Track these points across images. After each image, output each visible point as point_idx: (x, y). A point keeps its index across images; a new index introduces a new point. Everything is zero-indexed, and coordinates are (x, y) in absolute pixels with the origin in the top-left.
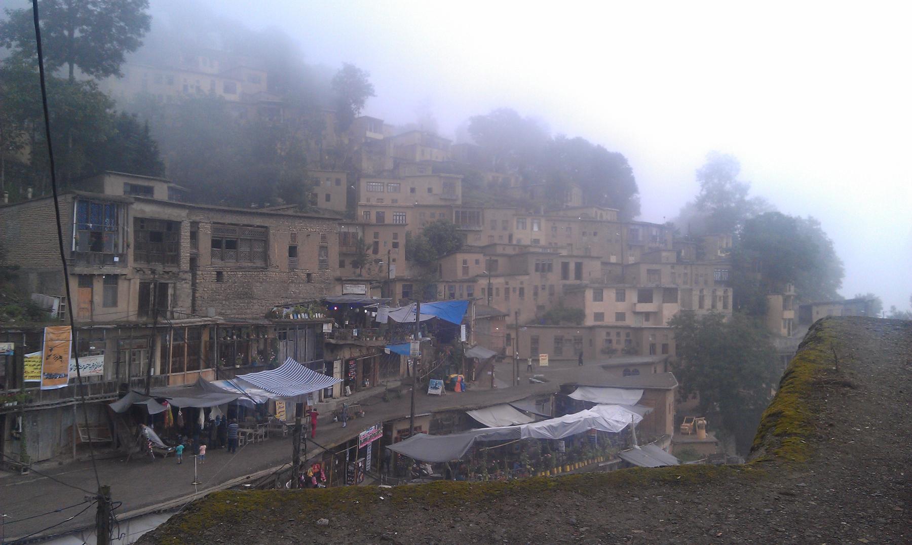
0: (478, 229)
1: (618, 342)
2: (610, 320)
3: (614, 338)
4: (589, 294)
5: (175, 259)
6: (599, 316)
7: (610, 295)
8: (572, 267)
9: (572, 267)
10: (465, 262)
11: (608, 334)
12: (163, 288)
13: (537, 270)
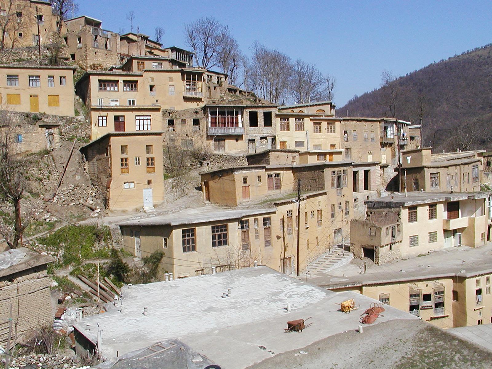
4: (405, 213)
7: (422, 212)
8: (361, 176)
10: (245, 180)
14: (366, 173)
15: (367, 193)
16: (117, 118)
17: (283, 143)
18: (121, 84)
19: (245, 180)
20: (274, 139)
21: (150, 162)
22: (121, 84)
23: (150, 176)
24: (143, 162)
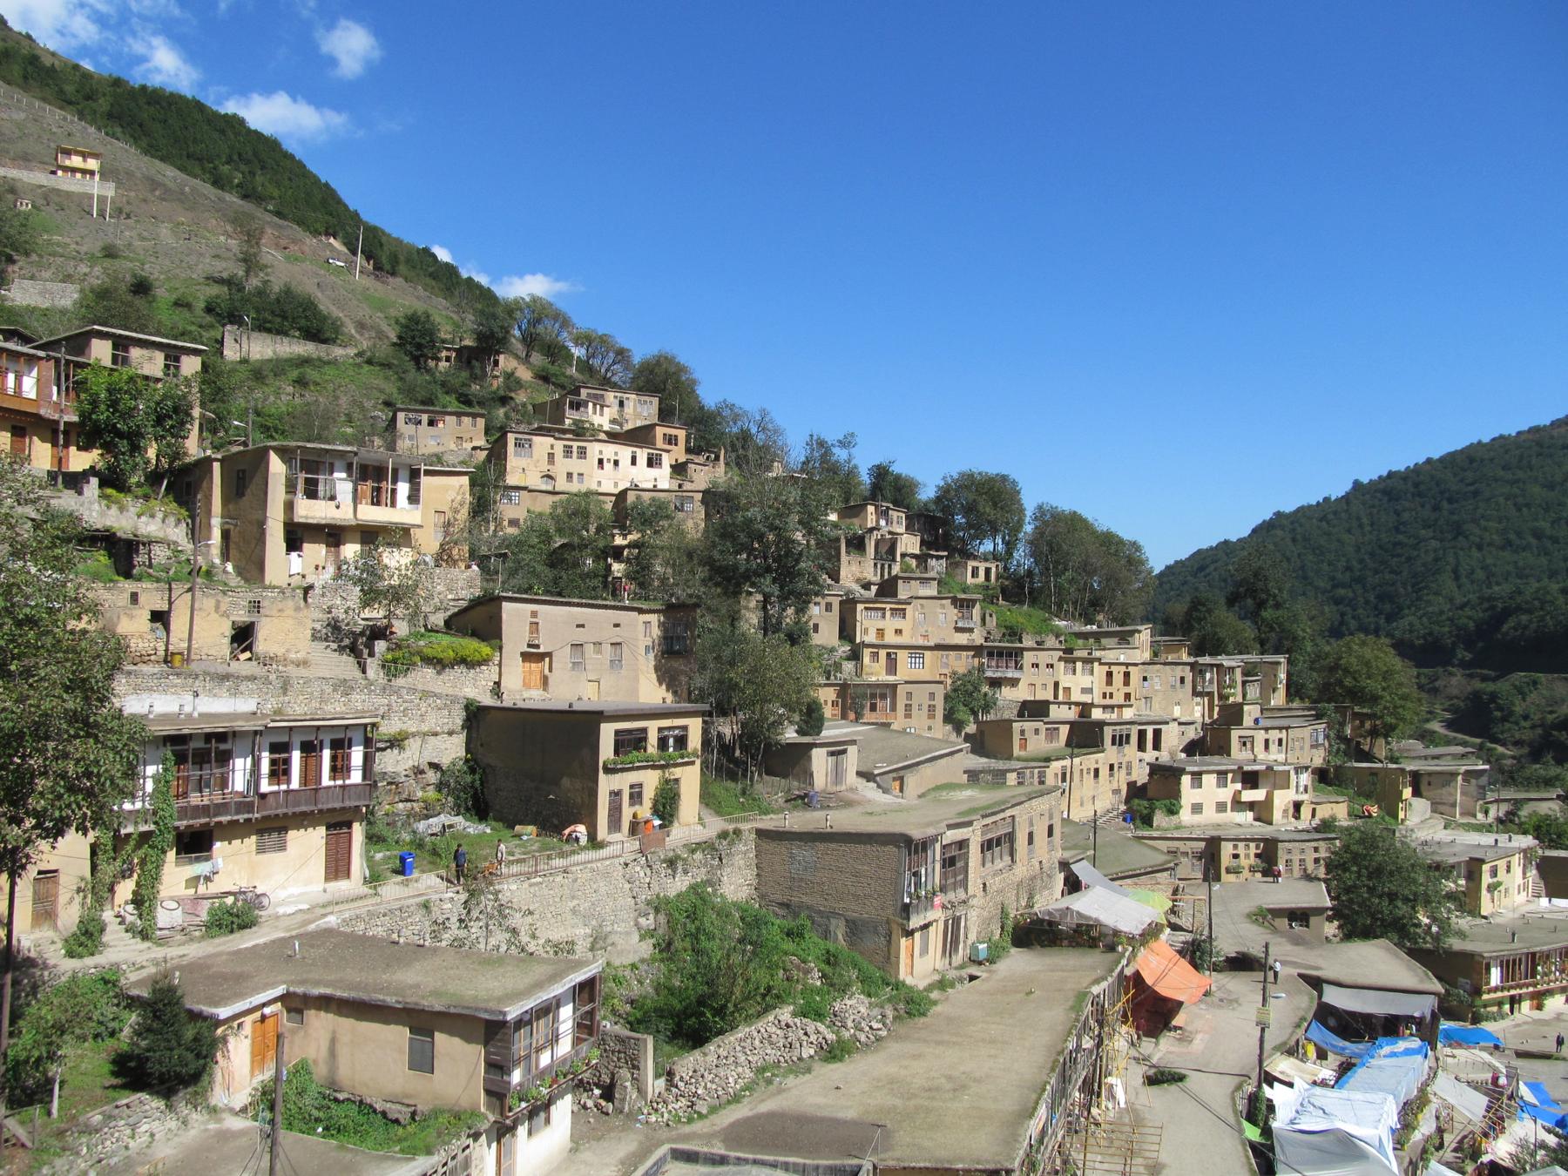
0: (1016, 675)
1: (1247, 856)
2: (1210, 815)
3: (1241, 850)
4: (1186, 780)
5: (964, 884)
6: (1197, 808)
7: (1209, 780)
8: (1150, 736)
9: (1150, 736)
10: (1022, 732)
11: (1235, 847)
12: (956, 921)
13: (1113, 743)
14: (1157, 733)
15: (1156, 753)
16: (888, 654)
17: (1067, 690)
18: (888, 614)
19: (1022, 732)
20: (1056, 685)
21: (932, 708)
22: (888, 614)
23: (930, 722)
24: (925, 708)
